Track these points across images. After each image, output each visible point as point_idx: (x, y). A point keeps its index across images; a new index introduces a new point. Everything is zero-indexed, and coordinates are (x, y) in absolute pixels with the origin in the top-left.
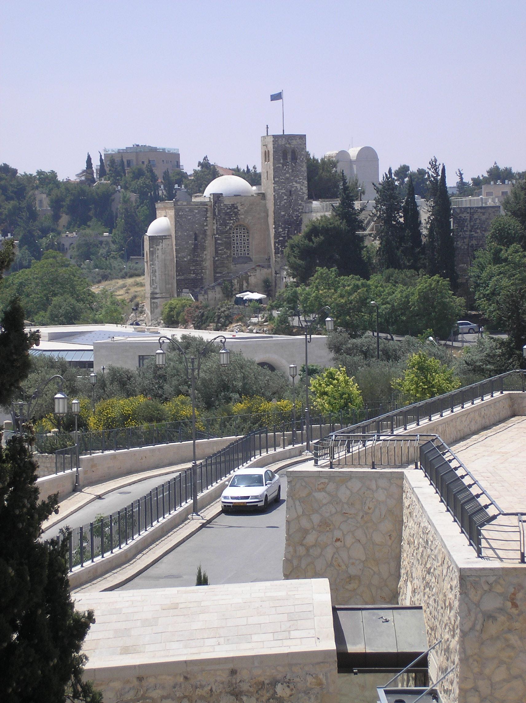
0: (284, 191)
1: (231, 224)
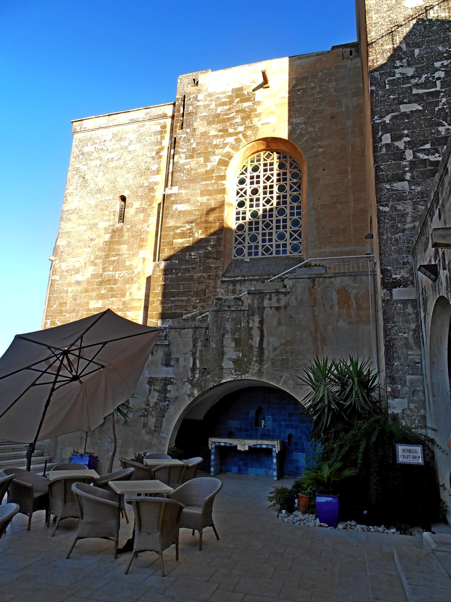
1: (227, 149)
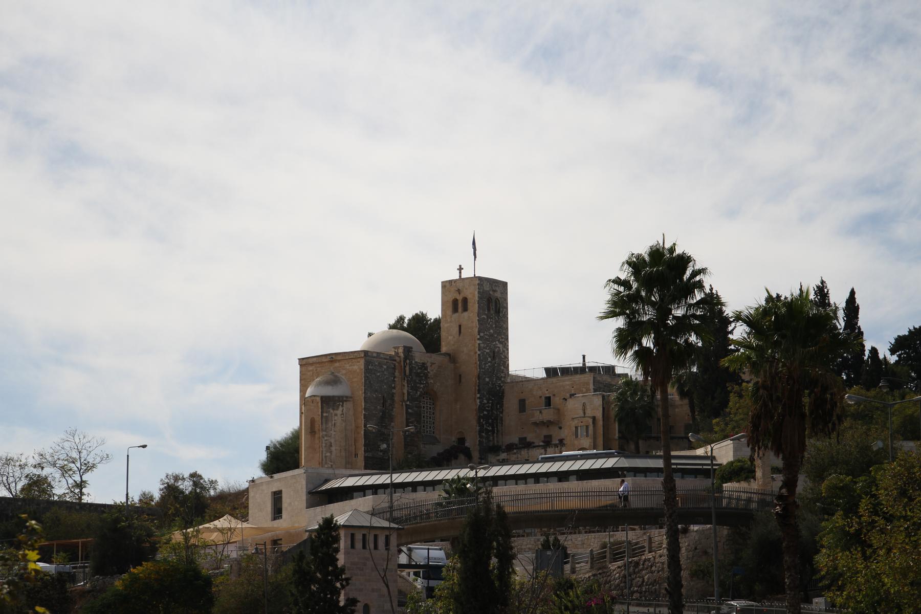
0: (488, 351)
1: (421, 390)
